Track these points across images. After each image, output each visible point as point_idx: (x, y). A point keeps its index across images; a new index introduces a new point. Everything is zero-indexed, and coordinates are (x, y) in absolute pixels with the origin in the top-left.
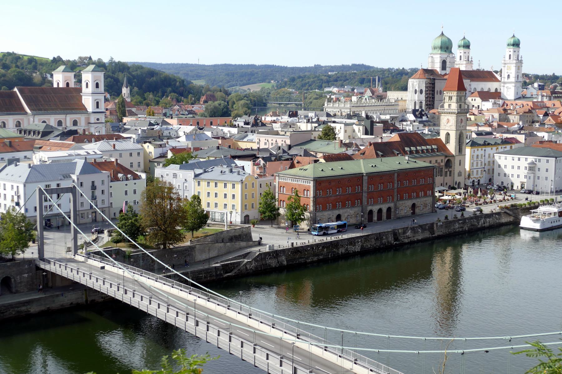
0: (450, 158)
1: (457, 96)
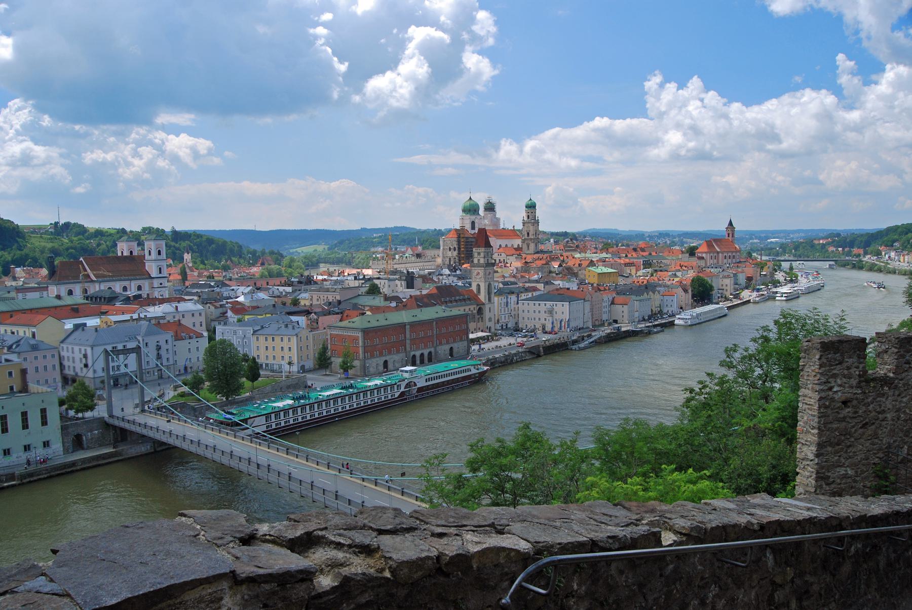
0: (482, 306)
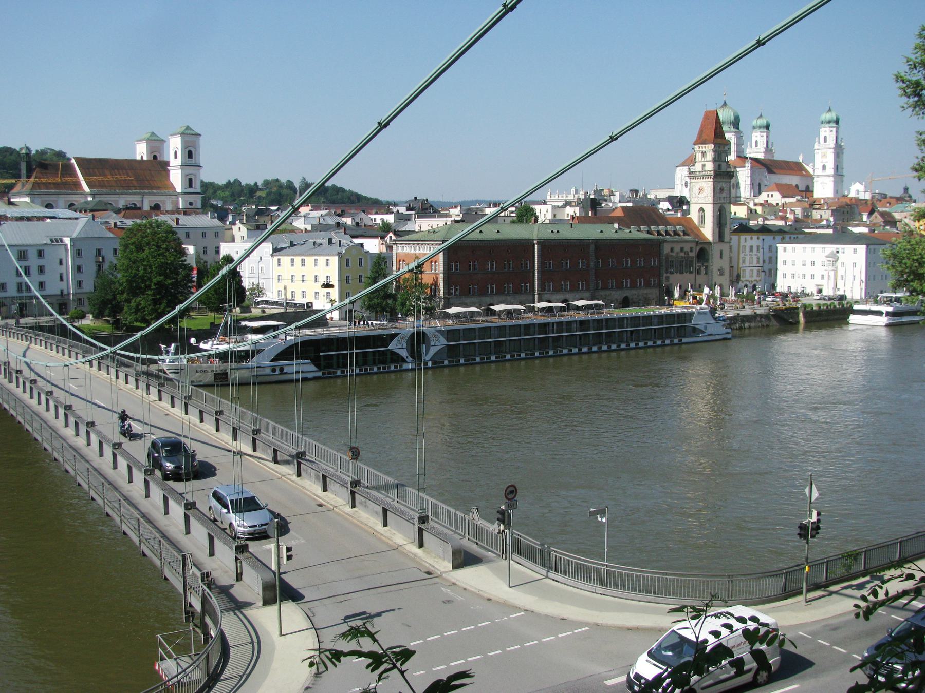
0: (706, 246)
1: (714, 151)
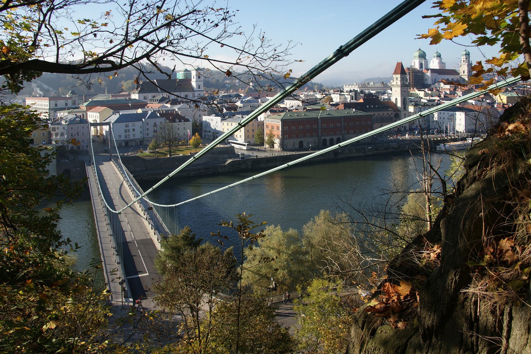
0: (398, 112)
